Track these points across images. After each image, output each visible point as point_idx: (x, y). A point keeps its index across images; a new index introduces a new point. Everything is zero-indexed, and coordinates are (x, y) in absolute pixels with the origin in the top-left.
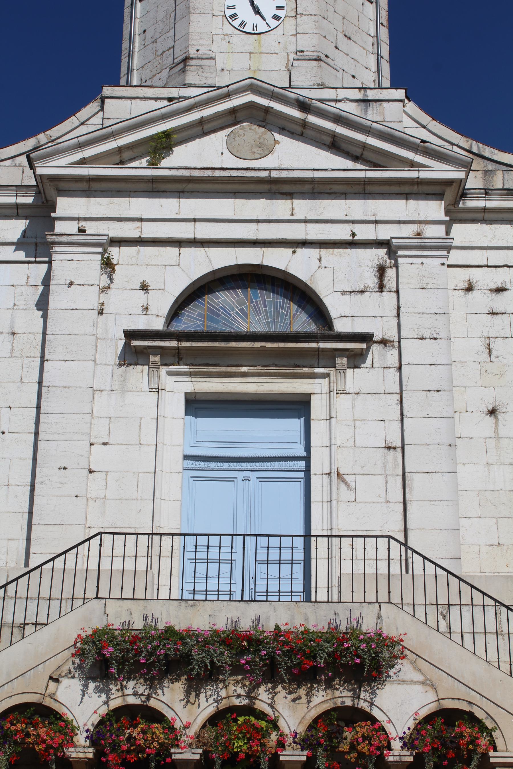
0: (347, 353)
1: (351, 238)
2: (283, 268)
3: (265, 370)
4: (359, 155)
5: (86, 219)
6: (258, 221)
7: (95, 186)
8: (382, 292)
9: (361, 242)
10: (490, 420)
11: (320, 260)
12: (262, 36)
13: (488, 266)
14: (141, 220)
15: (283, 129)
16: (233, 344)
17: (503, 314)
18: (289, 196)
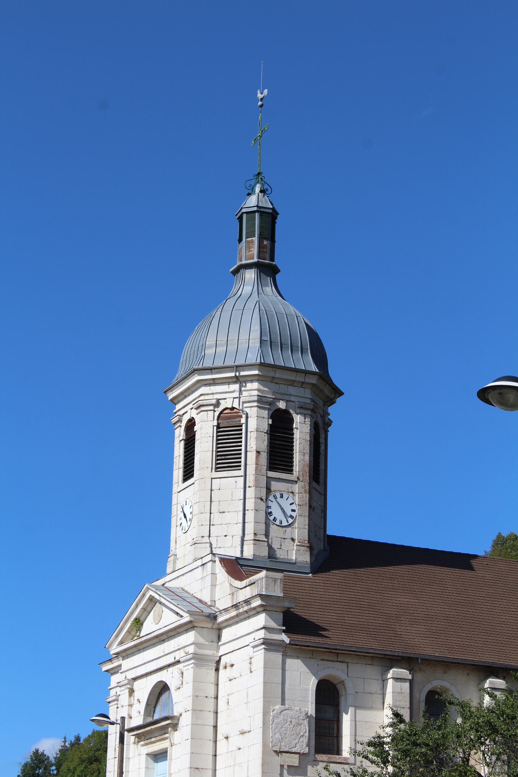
14: (135, 667)
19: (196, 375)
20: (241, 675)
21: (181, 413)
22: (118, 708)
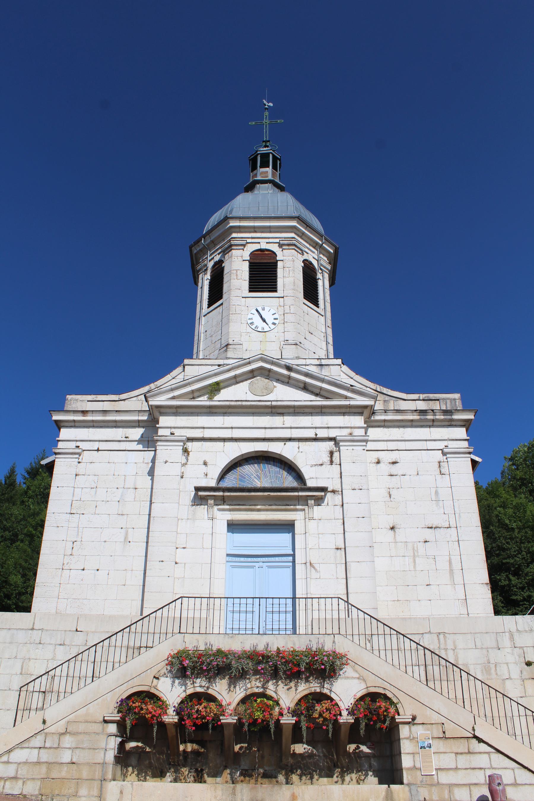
0: (314, 498)
1: (315, 436)
2: (279, 453)
3: (270, 507)
4: (318, 393)
5: (174, 428)
6: (265, 428)
7: (180, 410)
8: (332, 465)
9: (320, 438)
10: (391, 532)
11: (299, 448)
12: (266, 333)
13: (387, 450)
14: (204, 428)
15: (278, 380)
16: (253, 494)
17: (396, 475)
18: (282, 415)
19: (296, 221)
20: (418, 474)
21: (249, 240)
22: (79, 462)
